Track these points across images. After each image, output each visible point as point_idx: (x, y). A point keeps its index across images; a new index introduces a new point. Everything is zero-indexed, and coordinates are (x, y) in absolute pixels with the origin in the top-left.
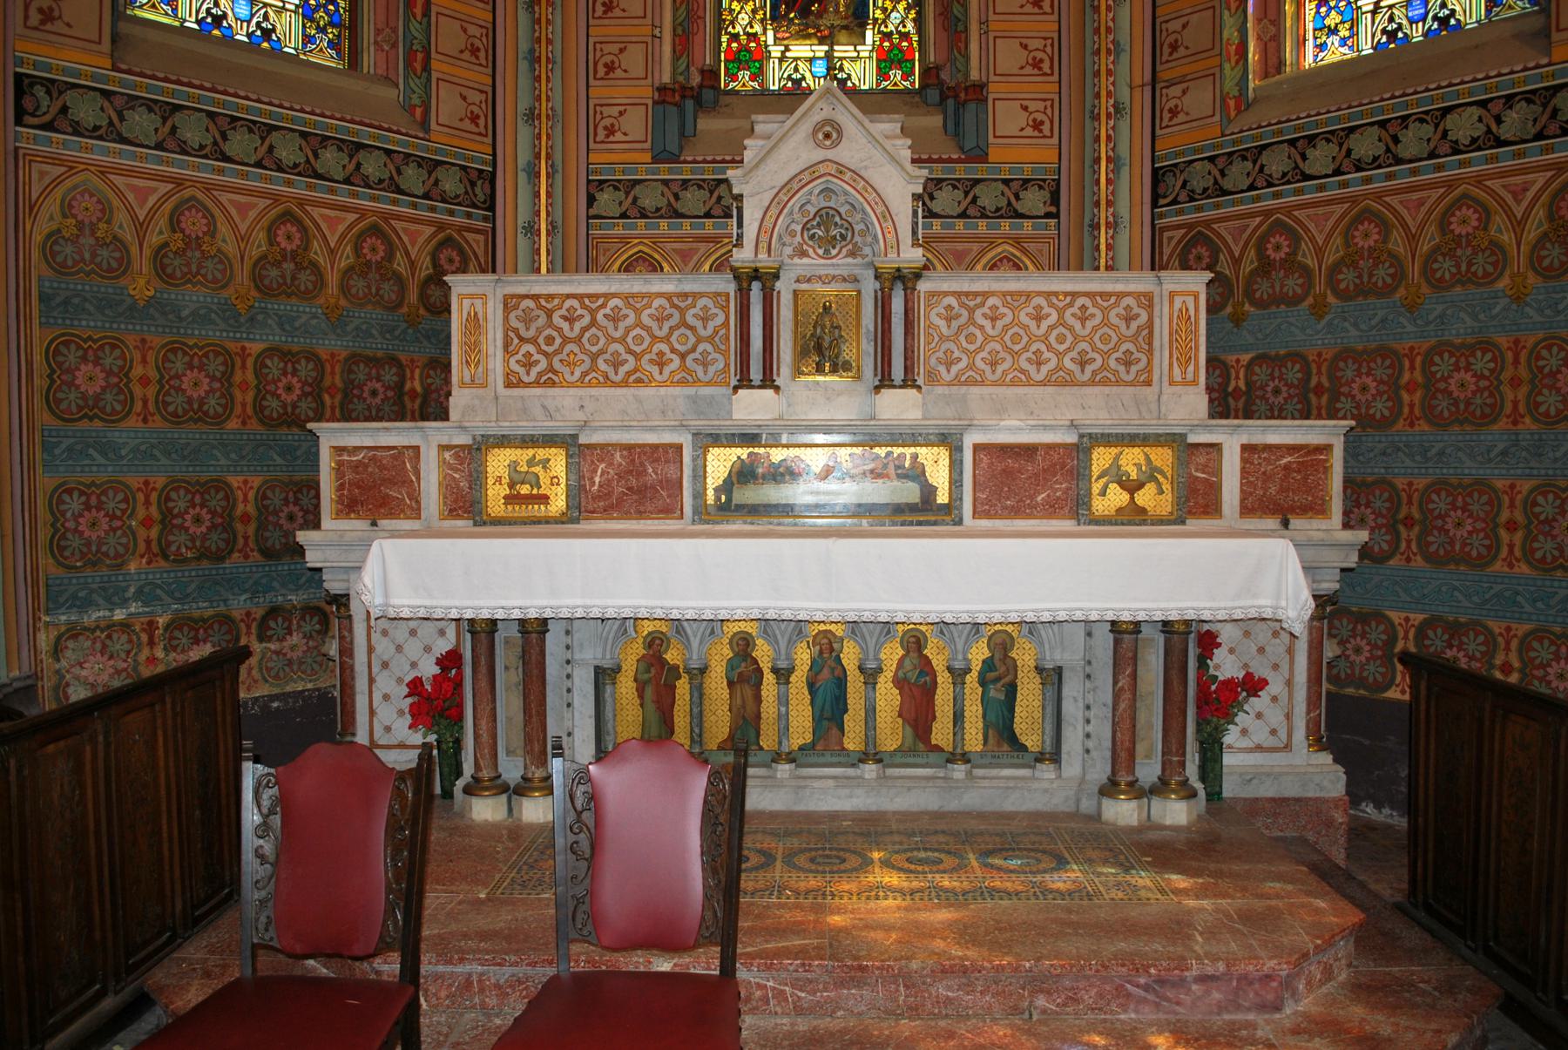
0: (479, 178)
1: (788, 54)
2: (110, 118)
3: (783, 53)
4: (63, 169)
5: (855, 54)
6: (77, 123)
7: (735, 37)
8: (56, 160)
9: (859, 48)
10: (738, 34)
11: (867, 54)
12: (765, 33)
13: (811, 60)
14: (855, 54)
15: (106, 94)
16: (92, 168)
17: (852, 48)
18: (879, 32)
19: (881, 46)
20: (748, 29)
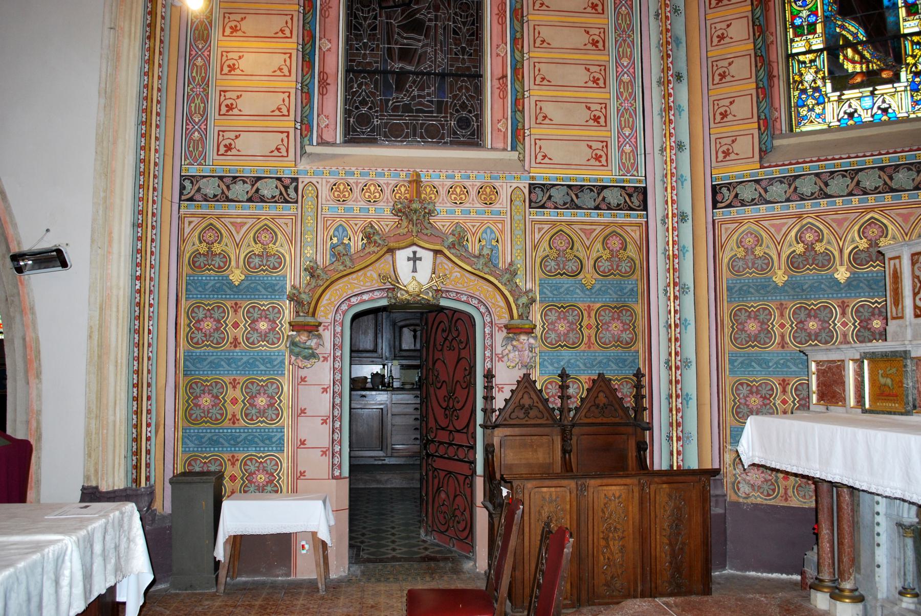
0: (635, 192)
1: (843, 97)
2: (760, 193)
3: (839, 97)
4: (737, 224)
5: (894, 90)
6: (743, 200)
7: (804, 91)
8: (733, 221)
9: (895, 85)
10: (806, 89)
11: (903, 89)
12: (825, 86)
13: (859, 99)
14: (894, 90)
15: (757, 181)
16: (751, 221)
17: (890, 86)
18: (911, 72)
19: (913, 81)
20: (813, 85)
